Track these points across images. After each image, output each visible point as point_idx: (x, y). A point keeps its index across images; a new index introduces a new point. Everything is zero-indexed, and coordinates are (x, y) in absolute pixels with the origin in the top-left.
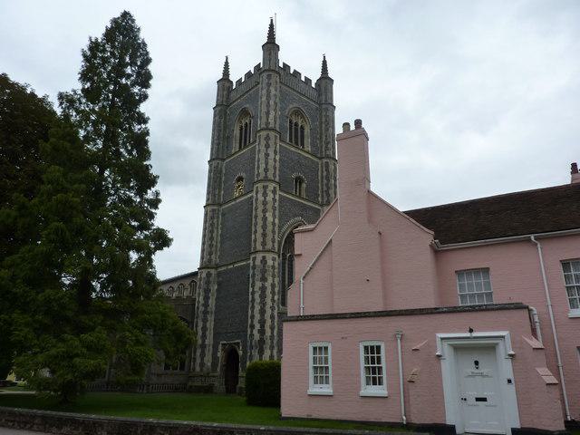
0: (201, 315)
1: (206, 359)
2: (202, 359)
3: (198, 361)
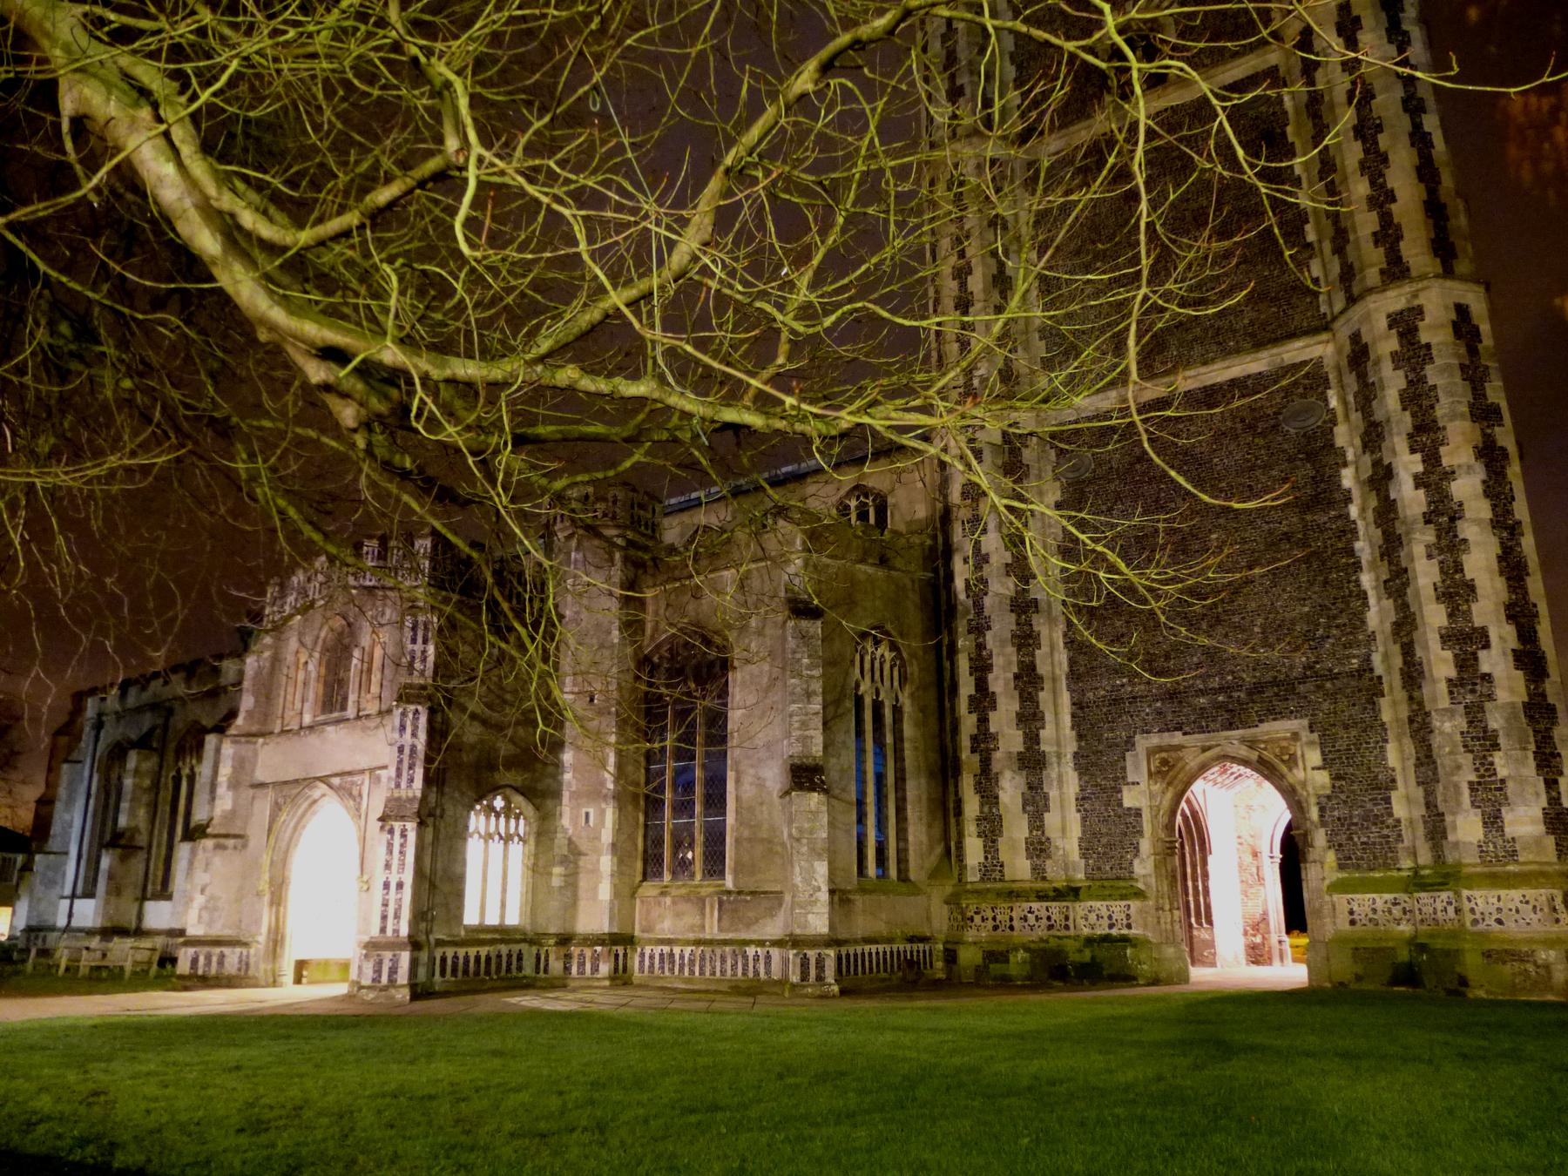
0: (1002, 626)
1: (1051, 820)
2: (1037, 822)
3: (1017, 829)
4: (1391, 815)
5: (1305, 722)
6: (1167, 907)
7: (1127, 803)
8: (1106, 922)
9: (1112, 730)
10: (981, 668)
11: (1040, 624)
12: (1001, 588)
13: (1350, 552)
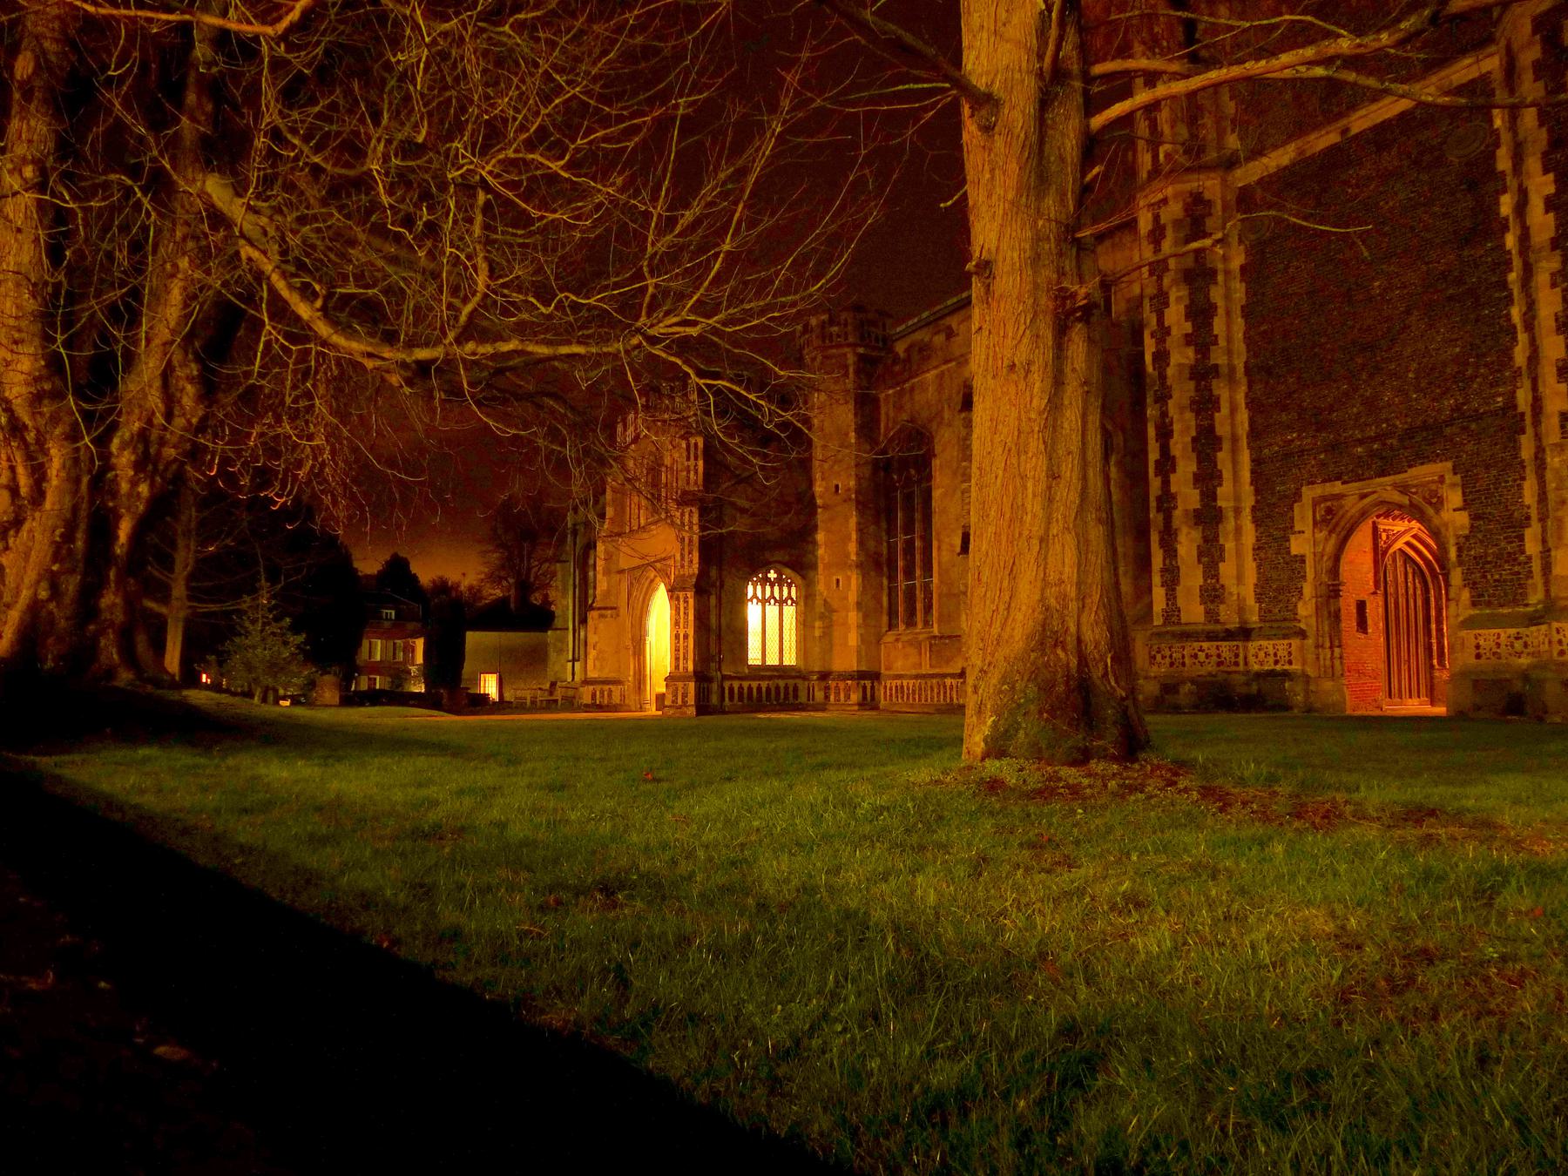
0: (1182, 393)
1: (1227, 570)
2: (1211, 570)
3: (1192, 578)
4: (1523, 552)
5: (1449, 465)
6: (1328, 644)
7: (1294, 551)
8: (1271, 659)
9: (1283, 483)
10: (1165, 434)
11: (1221, 389)
12: (1181, 357)
13: (1504, 285)
